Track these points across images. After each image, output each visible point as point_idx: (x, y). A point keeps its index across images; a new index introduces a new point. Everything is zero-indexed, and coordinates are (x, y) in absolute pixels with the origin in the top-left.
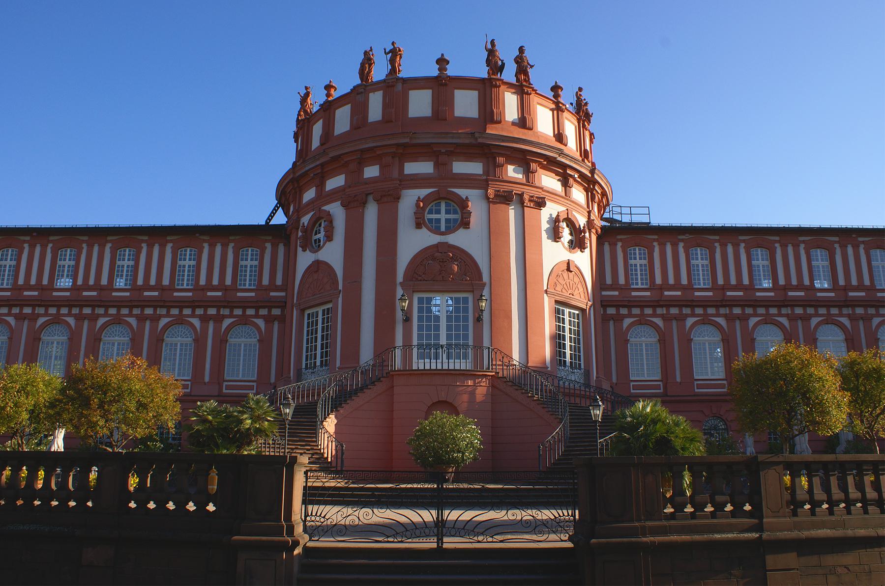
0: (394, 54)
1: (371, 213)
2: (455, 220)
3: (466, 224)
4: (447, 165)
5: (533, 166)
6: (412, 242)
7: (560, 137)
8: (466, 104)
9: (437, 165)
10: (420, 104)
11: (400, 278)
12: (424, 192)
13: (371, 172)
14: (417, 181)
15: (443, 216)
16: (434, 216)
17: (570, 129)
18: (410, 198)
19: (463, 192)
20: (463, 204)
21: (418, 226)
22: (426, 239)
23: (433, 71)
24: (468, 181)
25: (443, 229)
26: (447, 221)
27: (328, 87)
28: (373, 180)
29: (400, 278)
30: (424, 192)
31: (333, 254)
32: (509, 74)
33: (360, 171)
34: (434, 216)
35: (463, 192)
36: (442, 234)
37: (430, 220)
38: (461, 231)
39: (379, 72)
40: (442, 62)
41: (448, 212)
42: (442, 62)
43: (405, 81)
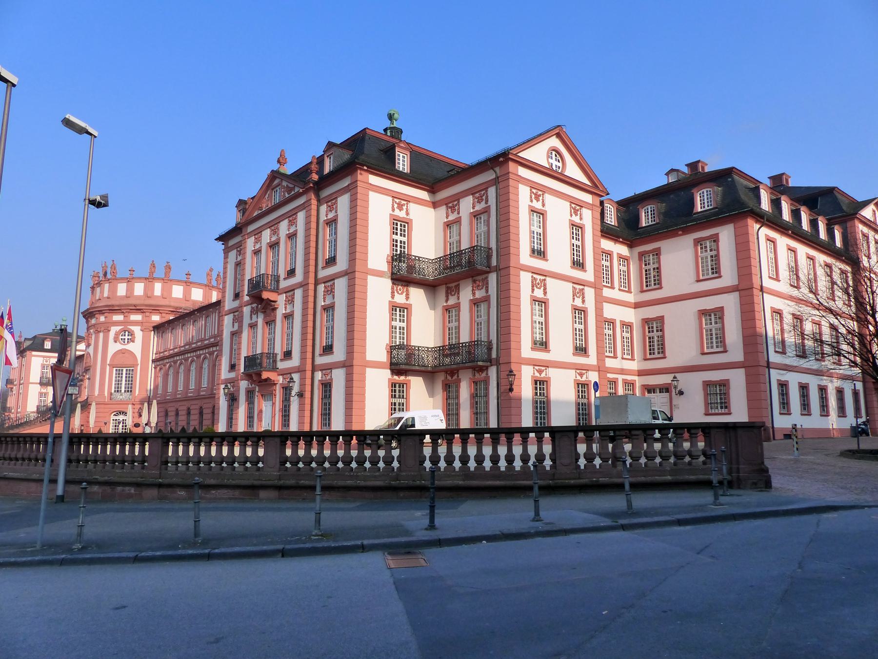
0: (114, 267)
1: (101, 335)
6: (114, 348)
10: (122, 289)
12: (118, 328)
13: (102, 319)
14: (117, 323)
15: (126, 337)
18: (114, 330)
19: (132, 328)
20: (131, 334)
21: (115, 342)
22: (119, 347)
23: (127, 275)
24: (135, 323)
30: (118, 328)
35: (132, 328)
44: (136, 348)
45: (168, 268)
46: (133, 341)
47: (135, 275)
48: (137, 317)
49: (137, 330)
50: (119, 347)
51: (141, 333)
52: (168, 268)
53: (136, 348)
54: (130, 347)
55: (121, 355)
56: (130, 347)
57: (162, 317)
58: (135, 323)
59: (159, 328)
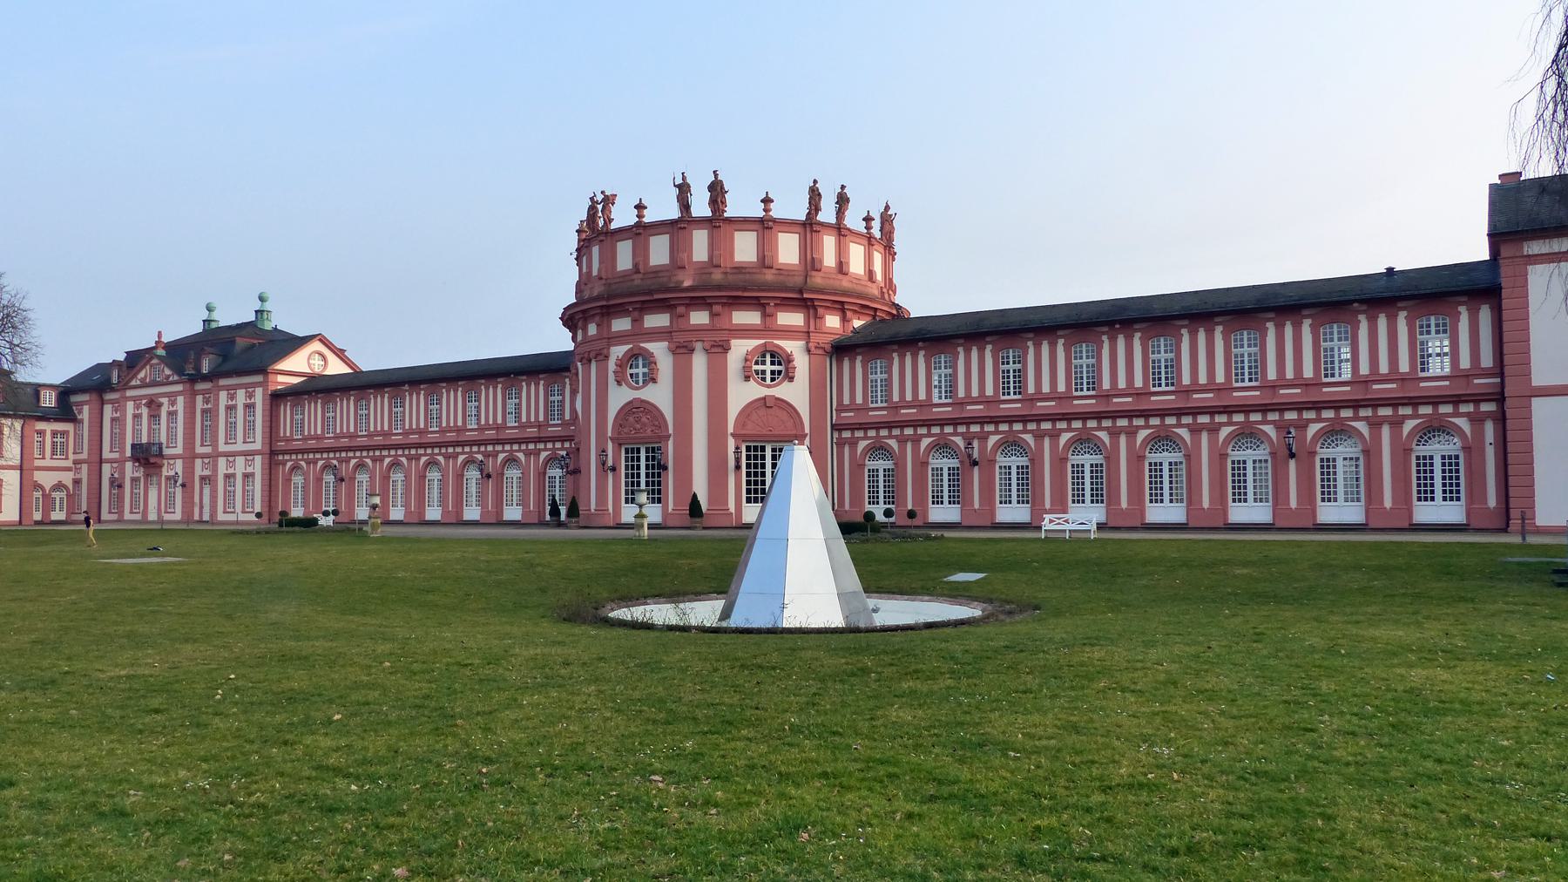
1: (699, 363)
2: (780, 372)
3: (791, 379)
4: (773, 316)
5: (849, 314)
6: (741, 394)
7: (870, 274)
8: (788, 250)
9: (765, 315)
11: (731, 429)
12: (753, 343)
13: (699, 318)
14: (746, 332)
15: (768, 367)
16: (760, 367)
17: (878, 258)
21: (747, 378)
22: (754, 391)
24: (789, 332)
25: (768, 381)
26: (773, 372)
27: (640, 207)
28: (699, 329)
29: (731, 429)
30: (753, 343)
31: (660, 395)
32: (827, 214)
33: (686, 316)
34: (760, 367)
36: (769, 386)
37: (757, 372)
38: (786, 383)
39: (701, 206)
40: (767, 201)
41: (773, 363)
42: (767, 201)
43: (730, 220)
44: (796, 393)
45: (842, 200)
46: (791, 379)
47: (776, 212)
48: (792, 319)
49: (793, 347)
50: (754, 391)
51: (806, 358)
52: (842, 200)
53: (796, 393)
54: (783, 391)
55: (762, 412)
56: (783, 391)
57: (844, 320)
58: (789, 332)
59: (842, 349)
